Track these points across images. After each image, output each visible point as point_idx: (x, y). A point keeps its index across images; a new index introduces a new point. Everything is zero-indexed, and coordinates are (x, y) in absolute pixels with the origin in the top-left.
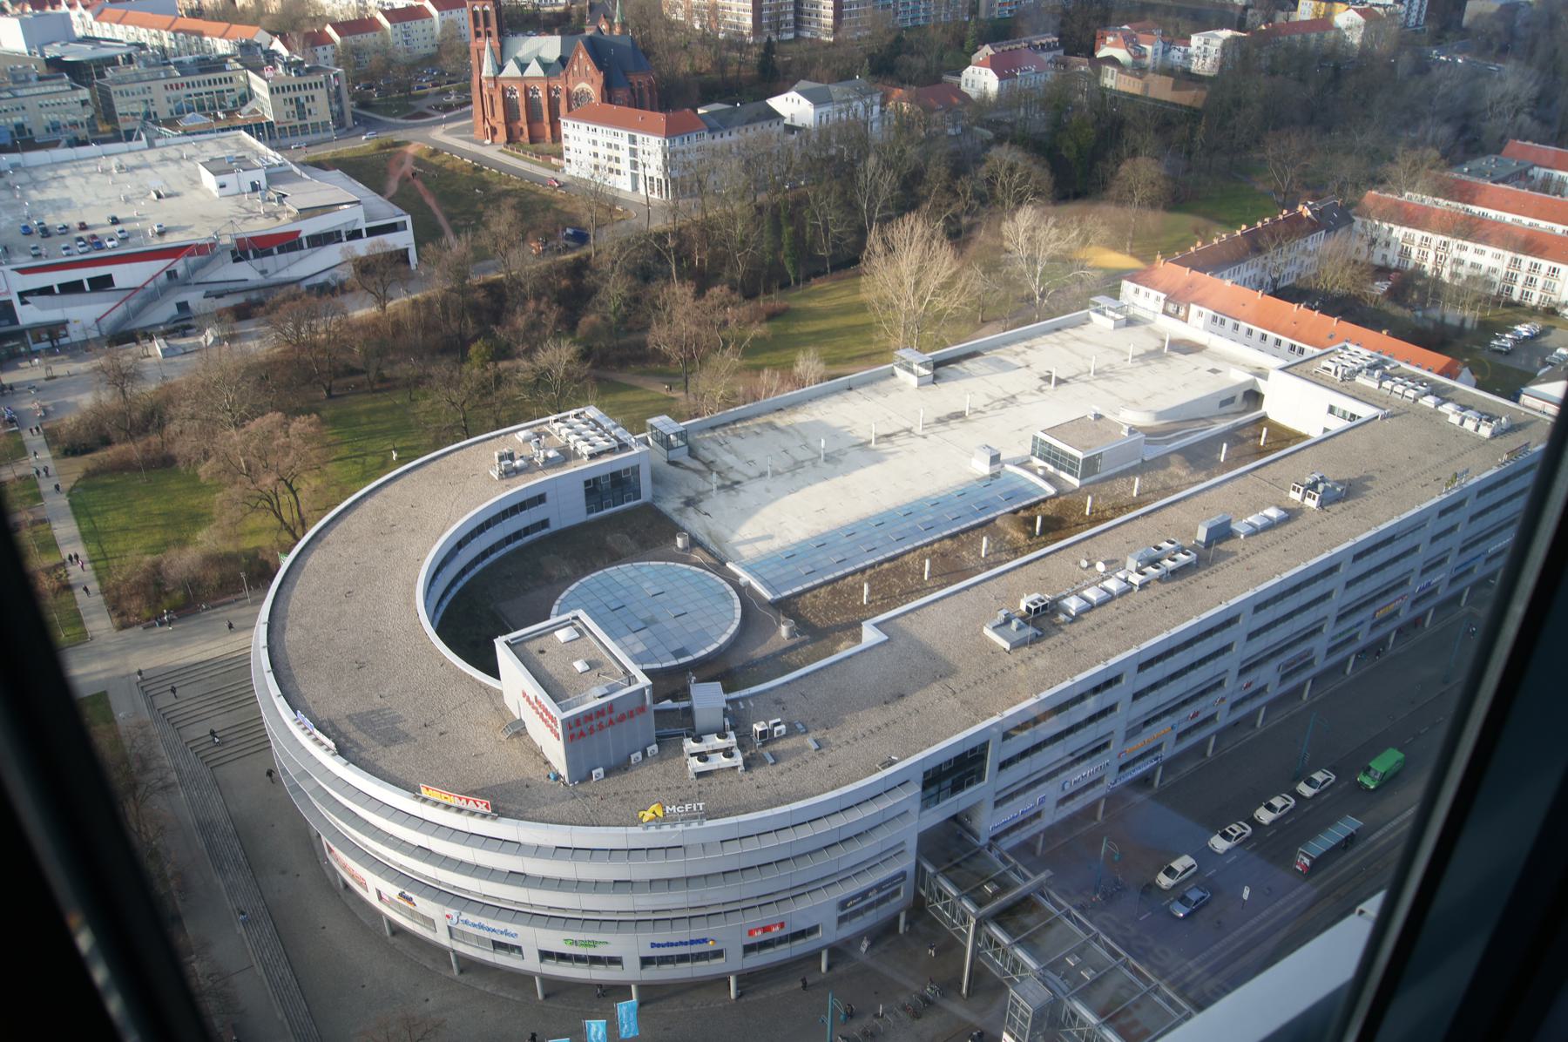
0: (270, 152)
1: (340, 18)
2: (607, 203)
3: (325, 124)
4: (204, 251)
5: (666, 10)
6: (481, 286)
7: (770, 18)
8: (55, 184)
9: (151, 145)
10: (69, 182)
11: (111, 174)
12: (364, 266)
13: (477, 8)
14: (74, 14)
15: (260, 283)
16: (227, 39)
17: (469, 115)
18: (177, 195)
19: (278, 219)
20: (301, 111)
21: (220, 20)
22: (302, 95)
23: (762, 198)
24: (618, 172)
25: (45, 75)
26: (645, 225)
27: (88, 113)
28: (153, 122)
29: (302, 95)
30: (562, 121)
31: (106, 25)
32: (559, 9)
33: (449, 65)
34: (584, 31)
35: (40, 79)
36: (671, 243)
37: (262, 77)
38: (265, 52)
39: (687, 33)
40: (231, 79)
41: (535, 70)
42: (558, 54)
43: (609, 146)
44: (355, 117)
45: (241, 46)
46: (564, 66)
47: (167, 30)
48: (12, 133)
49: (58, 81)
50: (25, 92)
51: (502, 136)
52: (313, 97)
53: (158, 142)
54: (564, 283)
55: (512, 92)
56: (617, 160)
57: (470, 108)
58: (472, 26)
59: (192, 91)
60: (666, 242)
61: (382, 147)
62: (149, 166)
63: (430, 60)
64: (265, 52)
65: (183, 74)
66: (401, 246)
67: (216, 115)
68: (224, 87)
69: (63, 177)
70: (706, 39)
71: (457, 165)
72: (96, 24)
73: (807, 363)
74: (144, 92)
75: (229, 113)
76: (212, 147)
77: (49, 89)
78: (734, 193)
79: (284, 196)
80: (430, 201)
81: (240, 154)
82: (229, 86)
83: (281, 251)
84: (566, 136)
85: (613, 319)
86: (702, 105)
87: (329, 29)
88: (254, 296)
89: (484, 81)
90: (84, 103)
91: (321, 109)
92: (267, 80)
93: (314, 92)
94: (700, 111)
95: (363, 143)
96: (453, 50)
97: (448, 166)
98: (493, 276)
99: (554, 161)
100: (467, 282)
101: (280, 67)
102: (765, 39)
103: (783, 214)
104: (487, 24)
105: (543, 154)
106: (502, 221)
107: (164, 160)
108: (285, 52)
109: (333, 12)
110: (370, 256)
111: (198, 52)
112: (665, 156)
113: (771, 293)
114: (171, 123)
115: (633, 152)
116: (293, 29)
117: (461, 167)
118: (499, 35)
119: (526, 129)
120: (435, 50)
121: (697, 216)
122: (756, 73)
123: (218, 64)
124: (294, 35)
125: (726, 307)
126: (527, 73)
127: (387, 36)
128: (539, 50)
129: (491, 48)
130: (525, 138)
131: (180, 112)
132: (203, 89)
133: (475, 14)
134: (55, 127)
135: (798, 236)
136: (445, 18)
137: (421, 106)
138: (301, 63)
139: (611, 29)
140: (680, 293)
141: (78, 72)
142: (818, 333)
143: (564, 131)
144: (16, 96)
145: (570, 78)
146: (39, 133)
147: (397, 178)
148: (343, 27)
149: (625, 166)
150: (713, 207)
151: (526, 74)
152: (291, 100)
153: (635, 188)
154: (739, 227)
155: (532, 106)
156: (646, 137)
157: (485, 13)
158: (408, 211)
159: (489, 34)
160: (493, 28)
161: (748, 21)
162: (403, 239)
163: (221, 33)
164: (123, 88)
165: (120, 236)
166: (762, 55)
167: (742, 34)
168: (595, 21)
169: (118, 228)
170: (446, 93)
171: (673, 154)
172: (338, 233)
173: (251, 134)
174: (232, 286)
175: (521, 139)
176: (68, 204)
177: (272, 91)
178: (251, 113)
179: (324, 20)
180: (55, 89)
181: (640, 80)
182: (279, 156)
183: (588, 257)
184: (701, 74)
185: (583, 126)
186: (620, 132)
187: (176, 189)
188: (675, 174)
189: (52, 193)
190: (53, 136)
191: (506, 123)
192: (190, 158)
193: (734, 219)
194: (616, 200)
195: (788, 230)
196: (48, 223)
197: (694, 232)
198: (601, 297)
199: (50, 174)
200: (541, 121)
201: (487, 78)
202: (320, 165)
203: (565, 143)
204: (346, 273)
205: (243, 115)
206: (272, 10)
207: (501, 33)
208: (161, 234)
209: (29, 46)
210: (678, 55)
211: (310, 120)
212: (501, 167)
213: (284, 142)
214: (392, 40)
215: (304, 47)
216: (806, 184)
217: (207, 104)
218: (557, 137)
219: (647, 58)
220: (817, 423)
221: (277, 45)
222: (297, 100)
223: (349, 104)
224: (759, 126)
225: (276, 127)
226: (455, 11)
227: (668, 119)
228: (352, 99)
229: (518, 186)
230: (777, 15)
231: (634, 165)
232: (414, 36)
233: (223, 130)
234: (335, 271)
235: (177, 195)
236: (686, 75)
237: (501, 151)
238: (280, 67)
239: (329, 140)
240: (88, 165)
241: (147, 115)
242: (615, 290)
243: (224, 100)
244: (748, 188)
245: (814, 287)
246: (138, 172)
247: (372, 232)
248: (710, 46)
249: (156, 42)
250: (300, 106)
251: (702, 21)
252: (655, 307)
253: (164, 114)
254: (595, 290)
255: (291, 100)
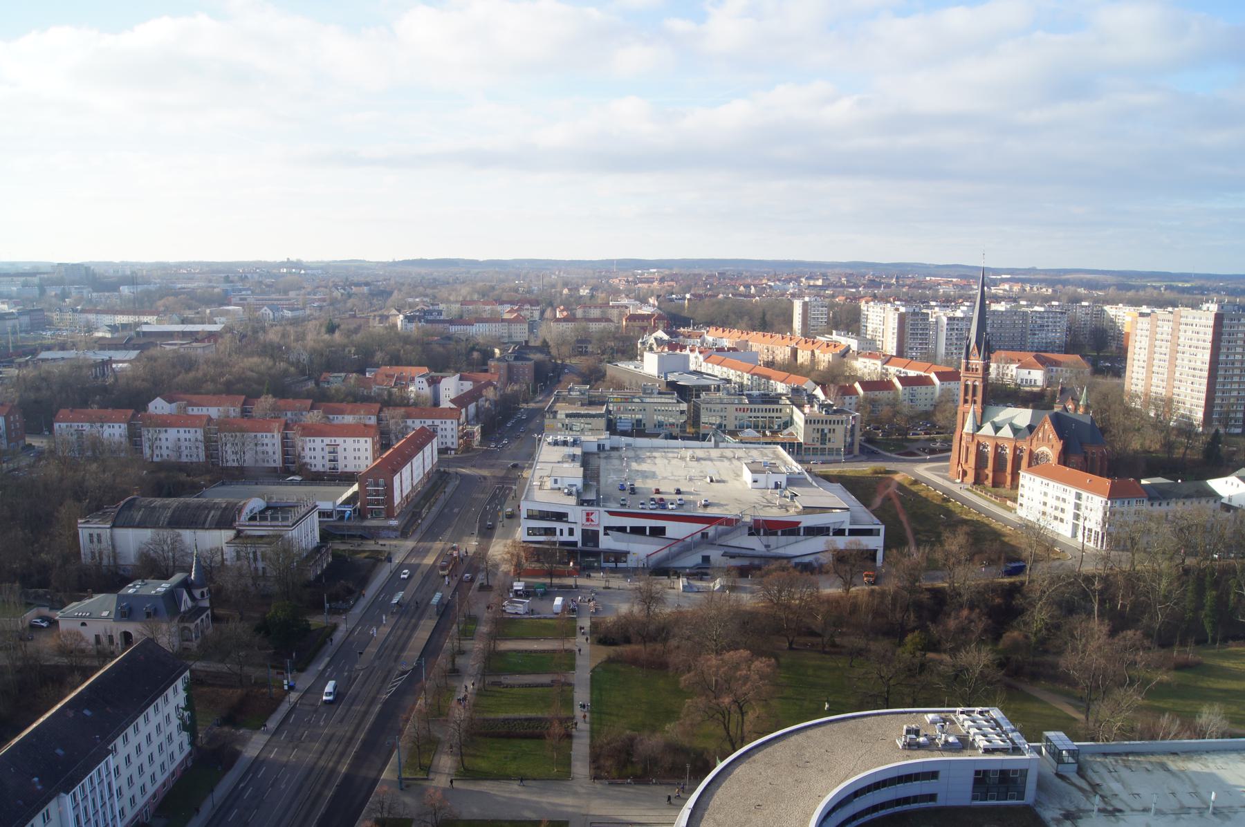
0: (794, 463)
1: (867, 378)
2: (1047, 545)
3: (838, 450)
4: (730, 523)
5: (1126, 399)
6: (927, 590)
7: (1220, 414)
8: (649, 461)
9: (716, 446)
10: (657, 461)
11: (685, 461)
12: (841, 557)
13: (969, 383)
14: (692, 356)
15: (763, 554)
16: (786, 383)
17: (947, 459)
18: (723, 481)
19: (787, 511)
20: (824, 438)
21: (784, 371)
22: (826, 428)
23: (1189, 561)
24: (1062, 520)
25: (664, 391)
26: (1077, 566)
27: (683, 419)
28: (722, 431)
29: (826, 428)
30: (1022, 473)
31: (710, 365)
32: (1035, 389)
33: (940, 419)
34: (1053, 408)
35: (660, 393)
36: (1097, 586)
37: (802, 412)
38: (808, 395)
39: (1142, 418)
40: (781, 410)
41: (1006, 432)
42: (1028, 423)
43: (1058, 498)
44: (862, 449)
45: (793, 390)
46: (1031, 432)
47: (747, 373)
48: (633, 424)
49: (670, 396)
50: (648, 400)
51: (970, 478)
52: (834, 430)
53: (721, 445)
54: (998, 601)
55: (985, 447)
56: (1063, 510)
57: (949, 454)
58: (962, 394)
59: (753, 414)
60: (1094, 584)
61: (876, 472)
62: (711, 460)
63: (927, 416)
64: (808, 395)
65: (751, 402)
66: (872, 547)
67: (764, 433)
68: (774, 415)
69: (655, 457)
70: (1159, 425)
71: (930, 494)
72: (704, 364)
73: (1210, 716)
74: (722, 411)
75: (774, 433)
76: (756, 454)
77: (663, 400)
78: (1164, 553)
79: (796, 495)
80: (903, 518)
81: (773, 462)
82: (778, 414)
83: (783, 534)
84: (1022, 486)
85: (1033, 639)
86: (1143, 478)
87: (857, 385)
88: (756, 562)
89: (964, 435)
90: (682, 412)
91: (838, 439)
92: (805, 414)
93: (835, 426)
94: (1143, 482)
95: (865, 468)
96: (945, 411)
97: (923, 494)
98: (939, 584)
99: (1009, 503)
100: (917, 584)
101: (816, 406)
102: (1214, 430)
103: (1208, 578)
104: (974, 395)
105: (1001, 497)
106: (955, 543)
107: (722, 457)
108: (821, 396)
109: (863, 374)
110: (847, 550)
111: (764, 390)
112: (1105, 514)
113: (1187, 646)
114: (733, 434)
115: (1077, 507)
116: (832, 382)
117: (934, 495)
118: (983, 404)
119: (991, 475)
120: (932, 409)
121: (1126, 567)
122: (1201, 457)
123: (775, 399)
124: (832, 386)
125: (1138, 649)
126: (1000, 434)
127: (898, 395)
128: (1012, 418)
129: (974, 412)
130: (989, 482)
131: (742, 427)
132: (760, 414)
133: (966, 386)
134: (660, 425)
135: (1221, 601)
136: (944, 387)
137: (913, 447)
138: (832, 406)
139: (1076, 409)
140: (1098, 627)
141: (683, 392)
142: (1226, 691)
143: (1021, 481)
144: (642, 402)
145: (1035, 442)
146: (649, 428)
147: (881, 497)
148: (867, 385)
149: (1069, 516)
150: (1141, 562)
151: (998, 435)
152: (818, 430)
153: (1074, 535)
154: (1164, 583)
155: (999, 458)
156: (1090, 496)
157: (975, 387)
158: (883, 522)
159: (975, 402)
160: (979, 398)
161: (1199, 415)
162: (875, 543)
163: (782, 379)
164: (709, 406)
165: (678, 502)
166: (1209, 443)
167: (1192, 424)
168: (1063, 401)
169: (679, 497)
170: (934, 440)
171: (1113, 514)
172: (828, 528)
173: (785, 449)
174: (744, 551)
175: (986, 482)
176: (653, 475)
177: (806, 422)
178: (788, 434)
179: (855, 378)
180: (667, 401)
181: (1093, 450)
182: (800, 467)
183: (1023, 583)
184: (1149, 452)
185: (1038, 480)
186: (1068, 488)
187: (724, 478)
188: (1112, 530)
189: (644, 467)
190: (657, 430)
191: (976, 469)
192: (739, 459)
193: (1160, 575)
194: (1054, 542)
195: (1210, 595)
196: (636, 486)
197: (1121, 580)
198: (1027, 618)
199: (648, 454)
200: (1005, 471)
201: (967, 434)
202: (828, 478)
203: (1021, 490)
204: (826, 559)
205: (782, 437)
206: (821, 368)
207: (985, 402)
208: (706, 506)
209: (660, 372)
210: (1131, 435)
211: (828, 445)
212: (964, 501)
213: (806, 458)
214: (901, 397)
215: (837, 395)
216: (1235, 558)
217: (760, 424)
218: (1015, 484)
219: (1103, 435)
220: (1212, 775)
221: (818, 392)
222: (823, 430)
223: (858, 437)
224: (1196, 503)
225: (804, 446)
226: (952, 383)
227: (1112, 485)
228: (863, 435)
229: (975, 518)
230: (1228, 413)
231: (1077, 517)
232: (918, 397)
233: (766, 443)
234: (818, 555)
235: (723, 481)
236: (1136, 452)
237: (967, 489)
238: (816, 406)
239: (839, 462)
240: (673, 452)
241: (720, 426)
242: (1040, 616)
243: (773, 423)
244: (1177, 552)
245: (1230, 649)
246: (703, 462)
247: (853, 532)
248: (1162, 431)
249: (738, 380)
250: (823, 435)
251: (1157, 410)
252: (1073, 636)
253: (731, 427)
254: (1021, 612)
255: (818, 430)
